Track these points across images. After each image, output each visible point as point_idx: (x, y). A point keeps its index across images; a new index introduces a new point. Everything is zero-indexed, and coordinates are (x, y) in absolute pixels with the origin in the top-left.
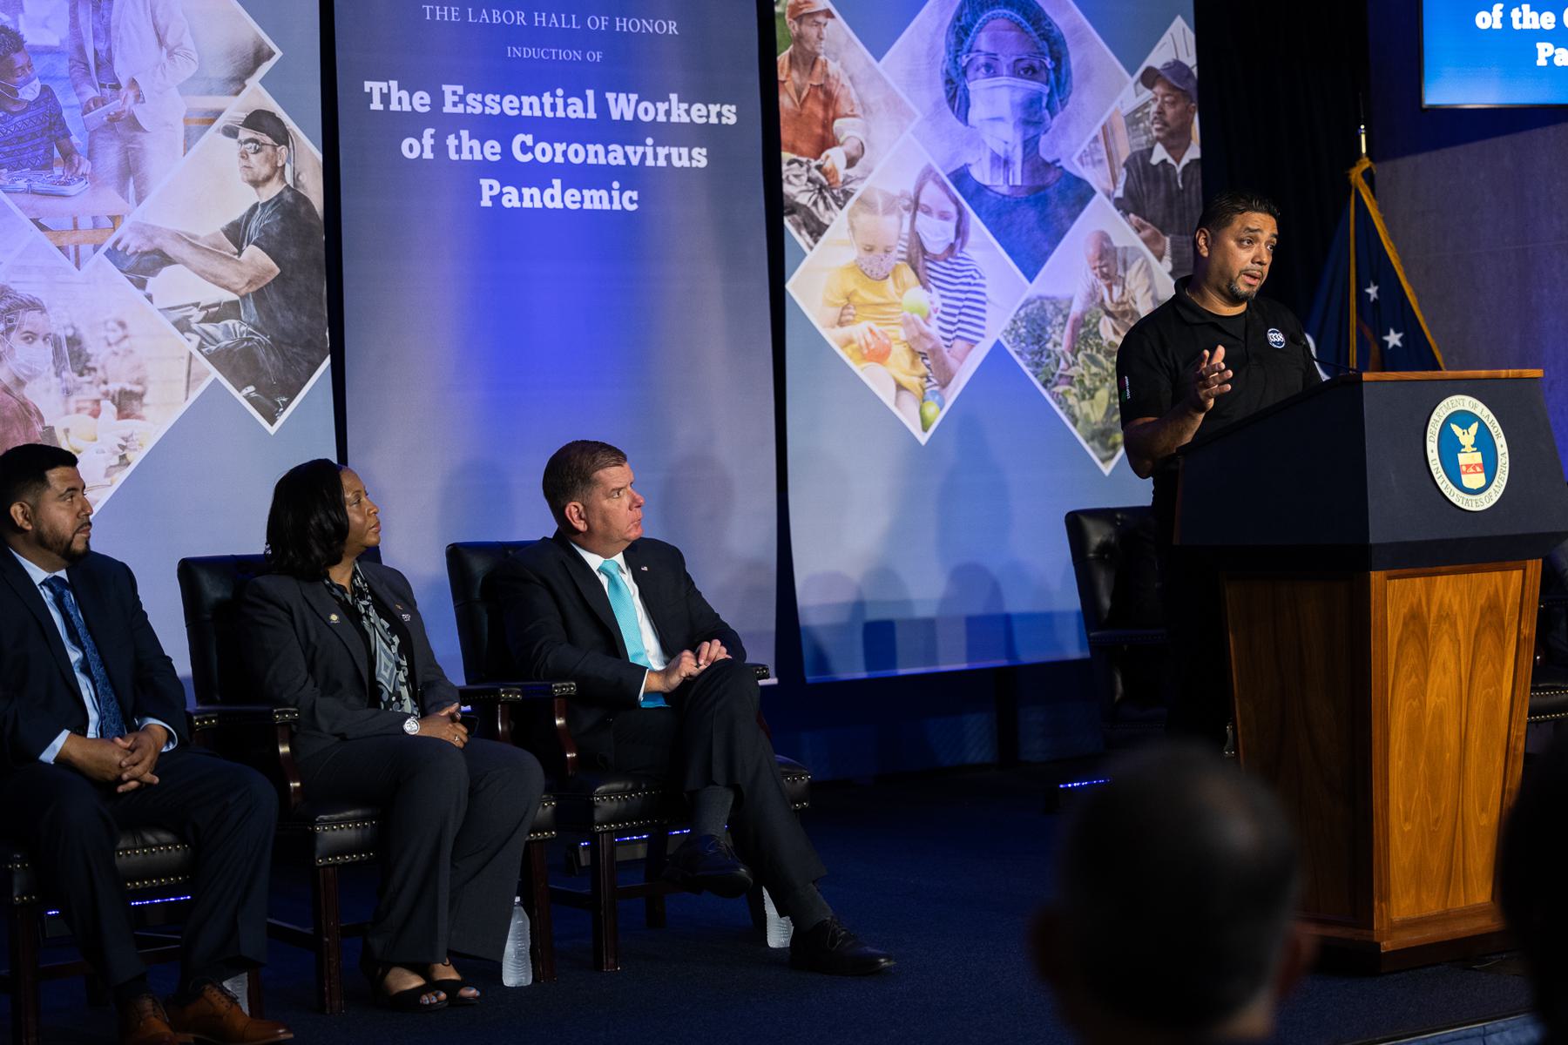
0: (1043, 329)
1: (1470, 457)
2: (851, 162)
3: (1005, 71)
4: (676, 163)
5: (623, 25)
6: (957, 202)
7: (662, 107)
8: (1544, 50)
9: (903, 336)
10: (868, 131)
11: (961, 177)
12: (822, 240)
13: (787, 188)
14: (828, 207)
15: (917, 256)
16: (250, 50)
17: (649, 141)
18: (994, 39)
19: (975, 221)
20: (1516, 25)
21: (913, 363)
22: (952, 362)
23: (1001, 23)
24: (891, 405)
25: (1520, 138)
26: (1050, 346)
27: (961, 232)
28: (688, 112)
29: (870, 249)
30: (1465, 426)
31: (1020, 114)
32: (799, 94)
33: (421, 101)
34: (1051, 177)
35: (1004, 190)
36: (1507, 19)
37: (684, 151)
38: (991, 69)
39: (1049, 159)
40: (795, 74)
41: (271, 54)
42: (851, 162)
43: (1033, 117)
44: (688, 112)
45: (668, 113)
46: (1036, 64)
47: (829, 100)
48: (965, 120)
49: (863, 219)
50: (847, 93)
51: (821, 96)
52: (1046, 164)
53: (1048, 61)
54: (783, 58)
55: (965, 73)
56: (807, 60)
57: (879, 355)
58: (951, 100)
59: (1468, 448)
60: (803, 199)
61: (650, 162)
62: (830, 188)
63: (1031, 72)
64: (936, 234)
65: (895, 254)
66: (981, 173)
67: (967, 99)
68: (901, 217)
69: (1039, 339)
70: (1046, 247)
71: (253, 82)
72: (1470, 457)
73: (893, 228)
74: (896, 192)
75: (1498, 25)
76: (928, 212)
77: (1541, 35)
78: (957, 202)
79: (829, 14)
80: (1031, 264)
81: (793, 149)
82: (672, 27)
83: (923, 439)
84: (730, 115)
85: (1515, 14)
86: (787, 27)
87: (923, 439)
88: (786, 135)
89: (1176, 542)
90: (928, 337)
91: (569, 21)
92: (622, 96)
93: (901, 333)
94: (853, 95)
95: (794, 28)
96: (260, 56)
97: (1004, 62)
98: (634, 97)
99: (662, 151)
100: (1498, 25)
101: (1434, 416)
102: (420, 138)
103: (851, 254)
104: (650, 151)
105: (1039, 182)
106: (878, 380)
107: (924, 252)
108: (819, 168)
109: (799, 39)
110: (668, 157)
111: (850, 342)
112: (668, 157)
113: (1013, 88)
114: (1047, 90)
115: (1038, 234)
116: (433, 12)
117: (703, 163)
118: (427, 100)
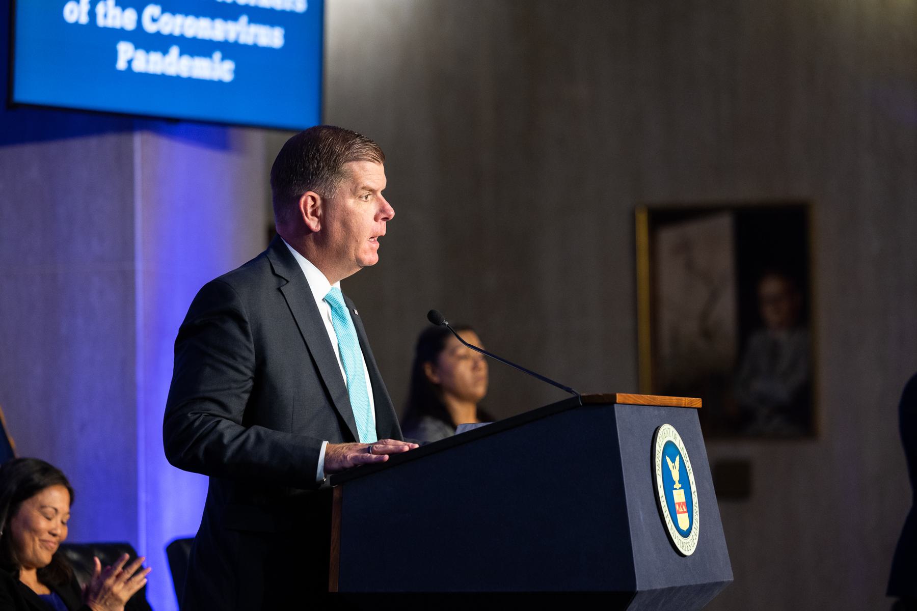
1: (679, 496)
8: (125, 50)
20: (101, 22)
25: (53, 148)
30: (673, 461)
36: (92, 14)
59: (677, 485)
72: (679, 496)
75: (84, 19)
77: (121, 34)
85: (100, 9)
89: (333, 586)
100: (84, 19)
101: (658, 448)
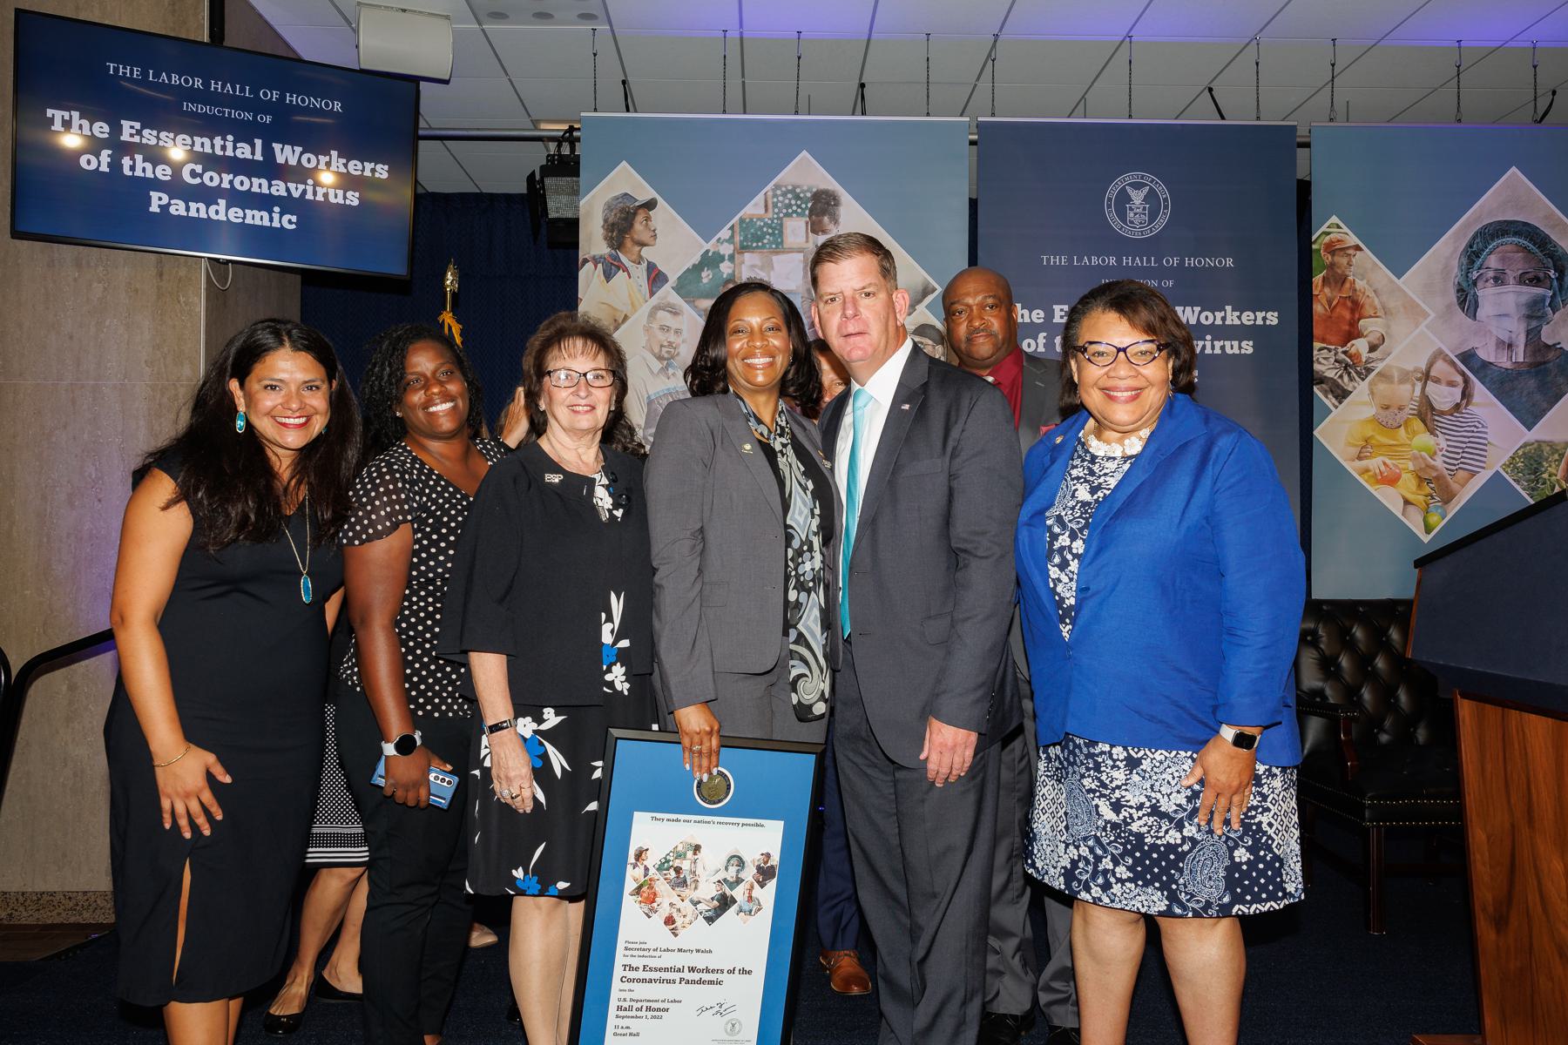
0: (1540, 464)
2: (1373, 348)
3: (1512, 281)
4: (1229, 351)
5: (1191, 262)
6: (1463, 374)
7: (1219, 315)
9: (1411, 466)
10: (1388, 327)
11: (1468, 357)
12: (1346, 402)
13: (1316, 367)
14: (1351, 379)
15: (1427, 413)
16: (920, 288)
17: (1209, 337)
18: (1503, 259)
19: (1479, 389)
21: (1419, 486)
22: (1455, 486)
23: (1509, 248)
24: (1400, 516)
26: (1545, 476)
27: (1466, 394)
28: (1239, 318)
29: (1387, 408)
31: (1524, 311)
32: (1330, 302)
33: (1038, 316)
34: (1551, 355)
35: (1508, 365)
37: (1236, 343)
38: (1499, 280)
39: (1550, 343)
40: (1327, 290)
41: (934, 290)
42: (1373, 348)
43: (1535, 313)
44: (1239, 318)
45: (1224, 319)
46: (1541, 275)
47: (1356, 307)
48: (1474, 317)
49: (1382, 387)
50: (1371, 301)
51: (1349, 304)
52: (1546, 346)
53: (1552, 273)
54: (1317, 279)
55: (1475, 283)
56: (1338, 279)
57: (1391, 480)
58: (1462, 303)
60: (1330, 374)
61: (1208, 351)
62: (1354, 366)
63: (1536, 281)
64: (1444, 397)
65: (1407, 410)
66: (1487, 353)
67: (1477, 302)
68: (1414, 385)
69: (1535, 471)
70: (1545, 405)
71: (921, 307)
73: (1408, 393)
74: (1410, 368)
76: (1437, 381)
78: (1463, 374)
79: (1358, 248)
80: (1530, 418)
81: (1323, 341)
82: (1229, 262)
83: (1426, 539)
84: (1273, 318)
86: (1322, 257)
87: (1426, 539)
88: (1317, 330)
90: (1433, 468)
91: (1149, 261)
92: (1188, 309)
93: (1411, 466)
94: (1376, 302)
95: (1328, 259)
96: (926, 291)
97: (1511, 275)
98: (1197, 309)
99: (1218, 344)
102: (1036, 339)
103: (1370, 411)
104: (1208, 344)
105: (1539, 359)
106: (1390, 498)
107: (1433, 409)
108: (1345, 353)
109: (1332, 266)
110: (1223, 348)
111: (1367, 471)
112: (1223, 348)
113: (1519, 293)
114: (1550, 293)
115: (1538, 397)
116: (1048, 260)
117: (1250, 351)
118: (1042, 314)
